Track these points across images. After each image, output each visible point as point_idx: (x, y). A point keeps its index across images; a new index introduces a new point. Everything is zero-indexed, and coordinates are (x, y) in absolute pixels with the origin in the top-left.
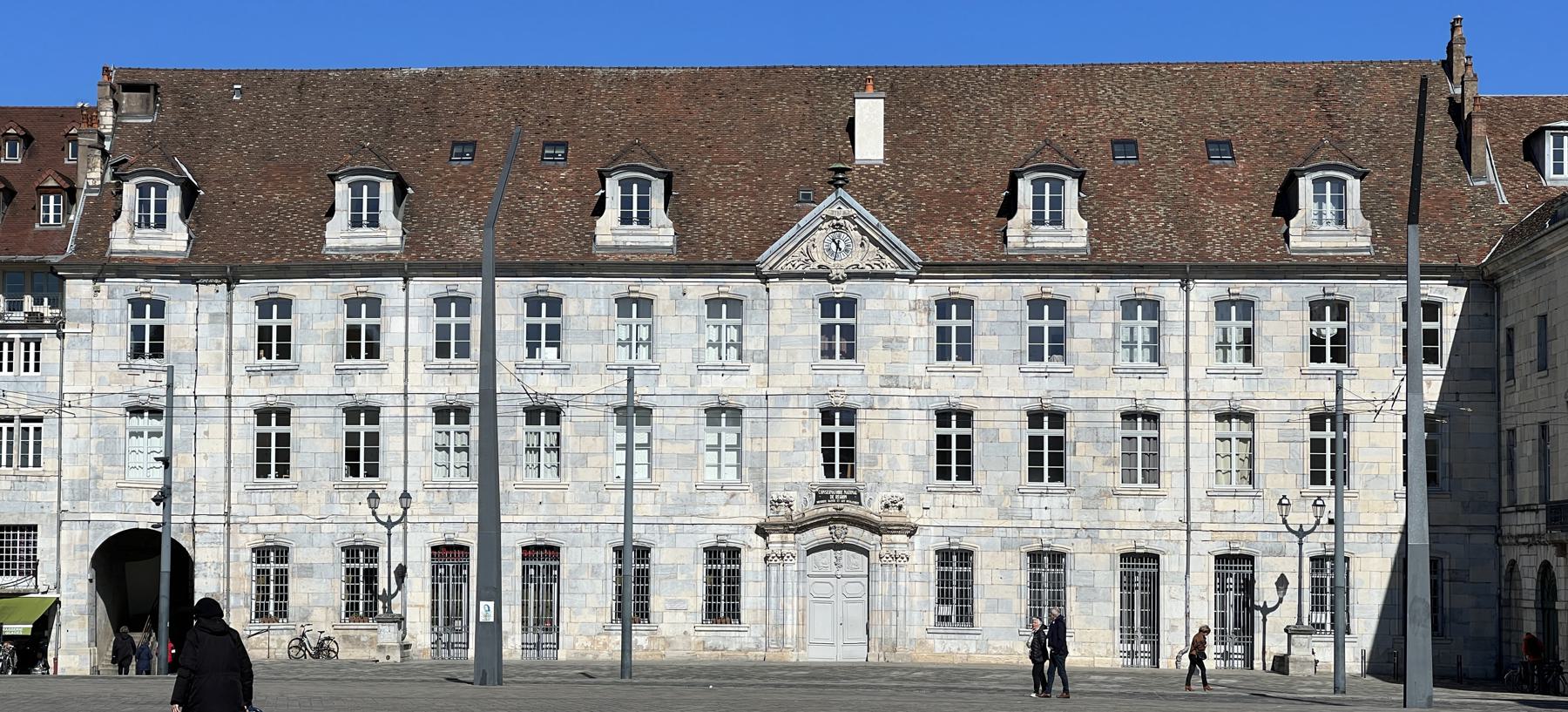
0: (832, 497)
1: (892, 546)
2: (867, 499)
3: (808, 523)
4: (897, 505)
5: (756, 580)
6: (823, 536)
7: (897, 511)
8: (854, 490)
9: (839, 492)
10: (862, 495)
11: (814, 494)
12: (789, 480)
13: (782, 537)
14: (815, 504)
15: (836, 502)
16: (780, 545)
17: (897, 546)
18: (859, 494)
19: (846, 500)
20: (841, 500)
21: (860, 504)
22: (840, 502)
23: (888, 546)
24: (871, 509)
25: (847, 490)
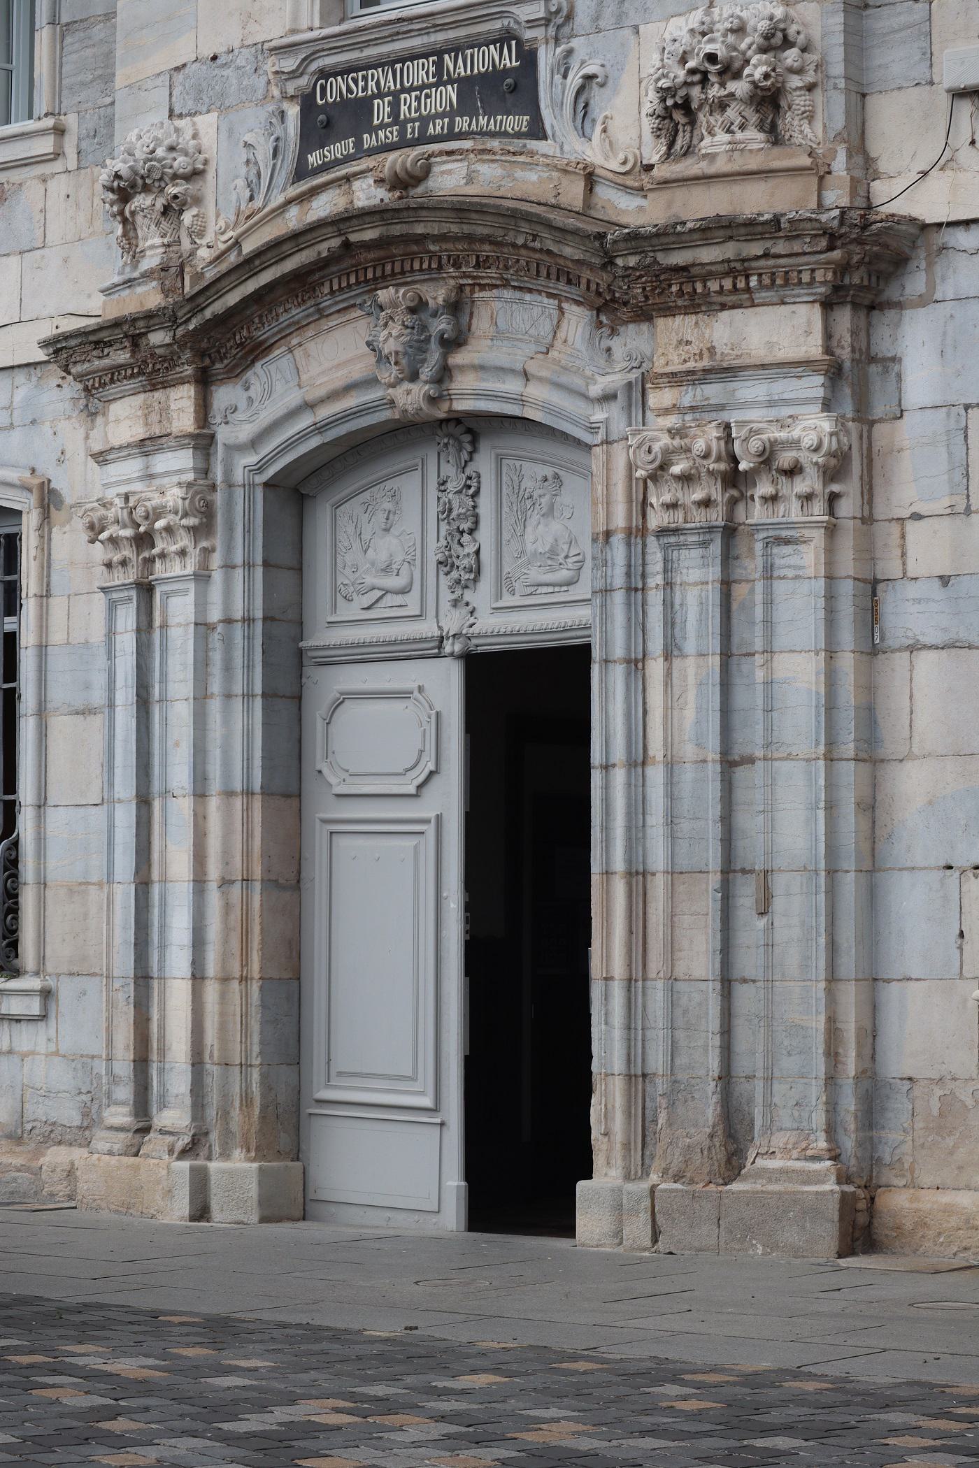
0: (382, 110)
1: (712, 392)
2: (574, 80)
3: (233, 298)
4: (739, 87)
5: (79, 704)
6: (339, 378)
7: (754, 137)
8: (504, 38)
9: (419, 72)
10: (546, 59)
11: (293, 111)
12: (184, 52)
13: (147, 409)
14: (301, 172)
15: (403, 143)
16: (131, 467)
17: (751, 390)
18: (529, 59)
19: (451, 114)
20: (425, 121)
21: (537, 131)
22: (424, 139)
23: (688, 396)
24: (593, 153)
25: (456, 49)
